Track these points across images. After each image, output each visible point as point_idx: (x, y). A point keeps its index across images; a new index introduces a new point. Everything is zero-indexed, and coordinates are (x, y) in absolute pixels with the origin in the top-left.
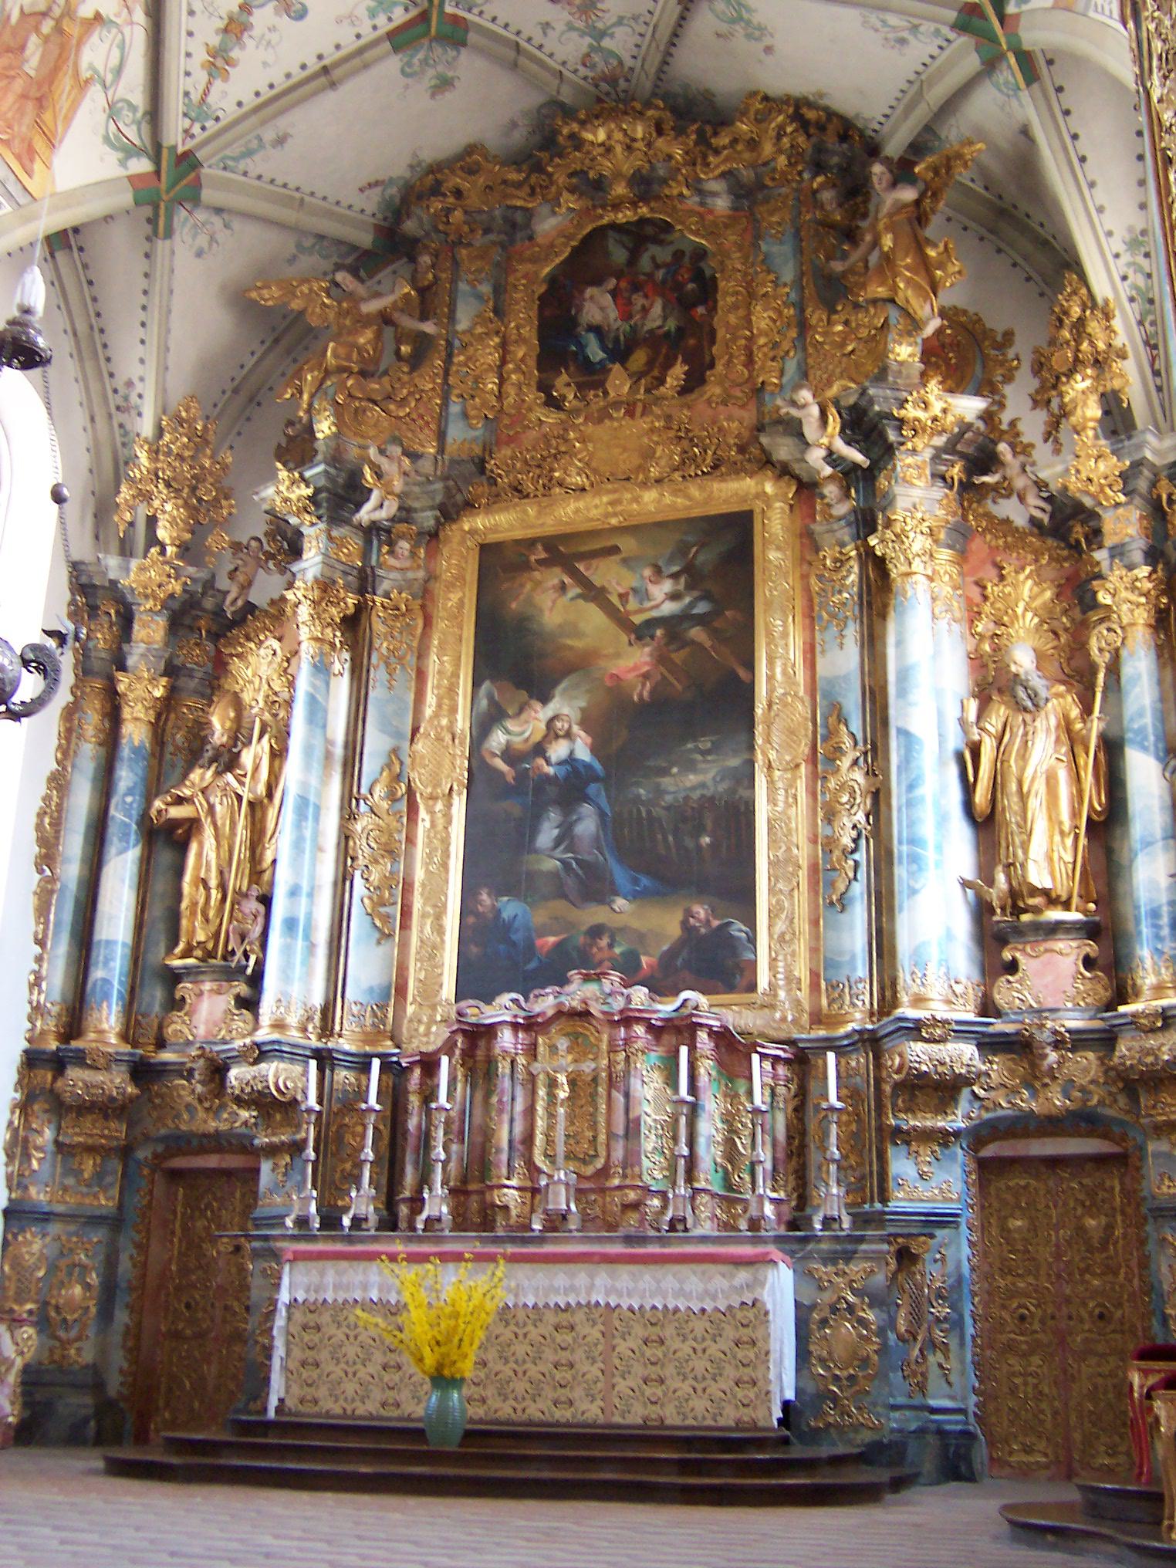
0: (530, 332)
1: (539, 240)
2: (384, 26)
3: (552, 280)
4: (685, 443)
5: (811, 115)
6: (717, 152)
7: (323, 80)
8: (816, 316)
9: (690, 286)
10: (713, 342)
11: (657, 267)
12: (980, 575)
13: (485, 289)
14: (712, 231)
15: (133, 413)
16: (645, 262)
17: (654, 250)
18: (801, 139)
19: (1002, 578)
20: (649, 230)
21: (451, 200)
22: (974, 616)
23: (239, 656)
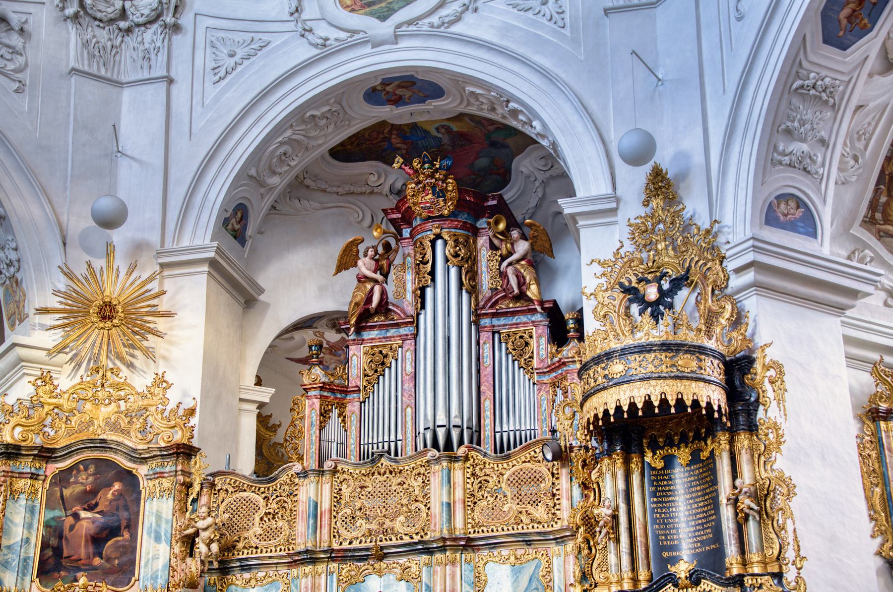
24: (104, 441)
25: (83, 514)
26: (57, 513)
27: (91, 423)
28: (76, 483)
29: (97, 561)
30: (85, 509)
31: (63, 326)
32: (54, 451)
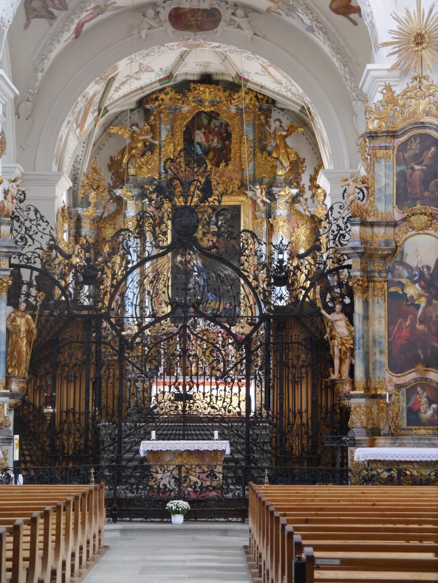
0: (181, 141)
1: (183, 112)
2: (158, 78)
3: (187, 126)
4: (225, 186)
5: (260, 97)
6: (234, 100)
7: (141, 91)
8: (259, 155)
9: (224, 134)
10: (230, 153)
11: (216, 127)
12: (293, 225)
13: (169, 127)
14: (231, 118)
15: (78, 163)
16: (212, 125)
17: (215, 121)
18: (257, 103)
19: (298, 227)
20: (213, 115)
21: (161, 102)
22: (291, 236)
23: (105, 228)
24: (422, 123)
25: (416, 167)
26: (402, 168)
27: (415, 113)
28: (411, 149)
29: (426, 194)
30: (417, 164)
31: (398, 51)
32: (395, 132)
